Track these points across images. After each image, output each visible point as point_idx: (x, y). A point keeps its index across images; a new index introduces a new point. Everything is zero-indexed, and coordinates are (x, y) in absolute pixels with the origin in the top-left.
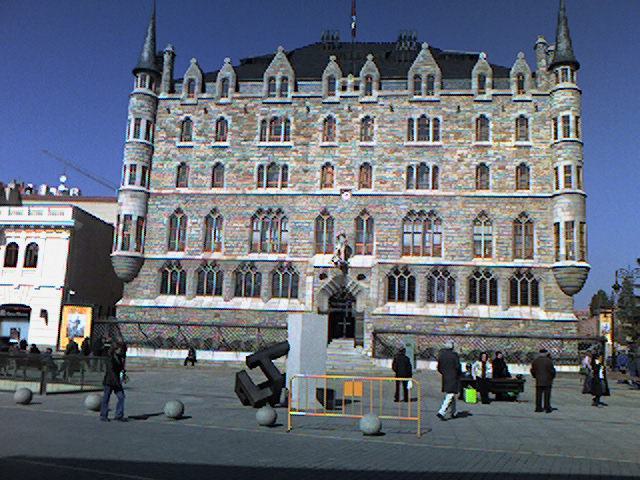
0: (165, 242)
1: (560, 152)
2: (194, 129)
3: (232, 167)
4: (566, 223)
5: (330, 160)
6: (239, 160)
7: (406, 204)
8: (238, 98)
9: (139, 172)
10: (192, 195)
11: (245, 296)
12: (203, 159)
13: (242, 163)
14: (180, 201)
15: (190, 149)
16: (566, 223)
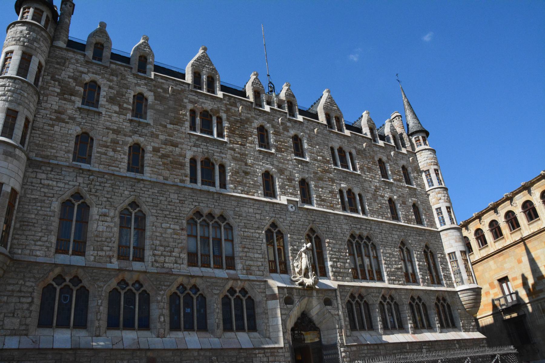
0: (53, 239)
1: (439, 195)
2: (103, 93)
3: (156, 150)
4: (461, 252)
5: (269, 166)
6: (166, 144)
7: (347, 224)
8: (162, 78)
9: (20, 124)
10: (102, 174)
11: (186, 329)
12: (117, 132)
13: (170, 148)
14: (80, 180)
15: (96, 117)
16: (461, 252)
